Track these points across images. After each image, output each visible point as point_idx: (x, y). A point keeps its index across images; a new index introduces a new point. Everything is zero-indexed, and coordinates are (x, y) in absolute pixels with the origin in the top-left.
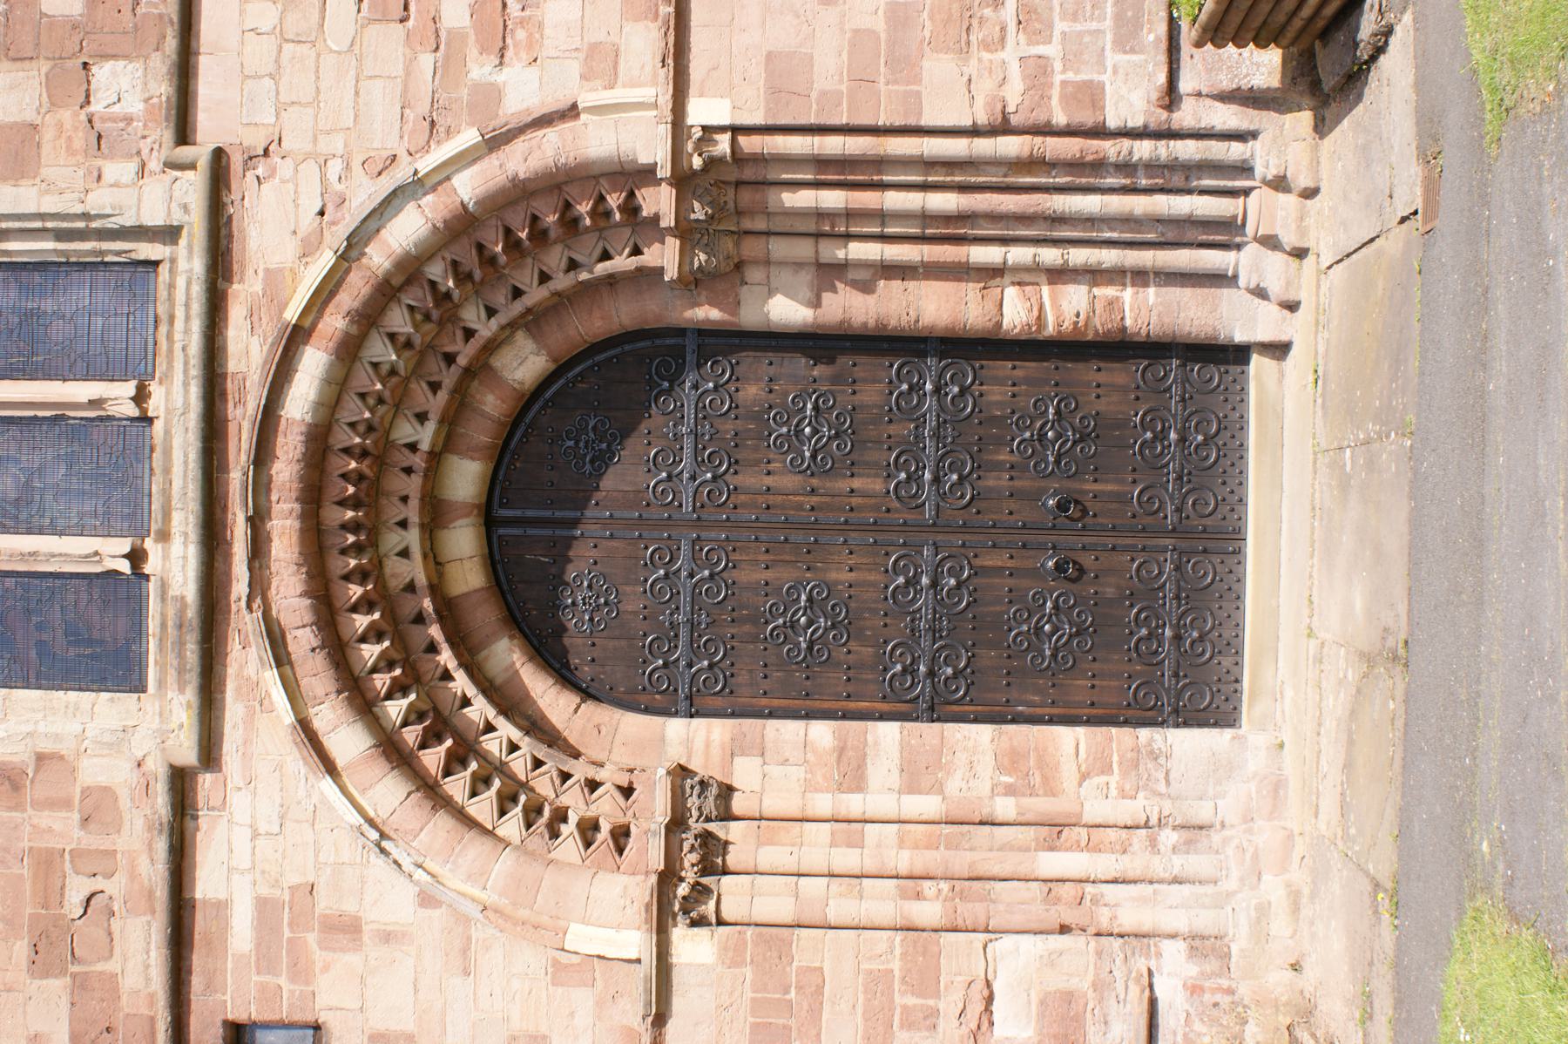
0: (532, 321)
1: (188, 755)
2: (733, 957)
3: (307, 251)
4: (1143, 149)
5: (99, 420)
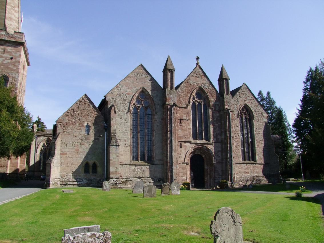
0: (205, 156)
1: (192, 142)
5: (203, 138)
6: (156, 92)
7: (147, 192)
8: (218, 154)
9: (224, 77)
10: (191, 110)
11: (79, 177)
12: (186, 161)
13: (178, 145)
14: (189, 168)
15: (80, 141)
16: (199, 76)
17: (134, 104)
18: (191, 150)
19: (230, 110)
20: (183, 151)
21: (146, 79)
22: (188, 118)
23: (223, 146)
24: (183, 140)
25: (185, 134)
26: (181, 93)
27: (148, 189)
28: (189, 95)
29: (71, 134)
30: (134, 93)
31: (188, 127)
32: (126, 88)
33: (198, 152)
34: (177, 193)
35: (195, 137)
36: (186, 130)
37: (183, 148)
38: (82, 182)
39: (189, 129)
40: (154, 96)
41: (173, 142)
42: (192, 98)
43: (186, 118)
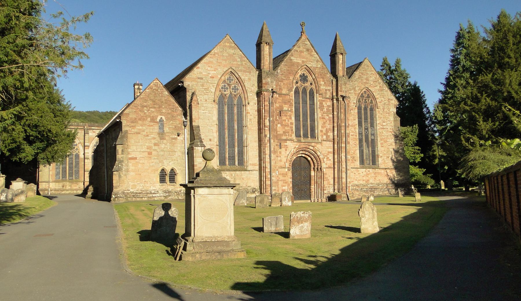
2: (286, 172)
3: (318, 148)
4: (323, 193)
6: (248, 74)
7: (259, 202)
8: (328, 156)
9: (339, 51)
10: (294, 98)
11: (154, 188)
12: (287, 165)
13: (277, 145)
14: (290, 174)
15: (153, 141)
16: (305, 50)
17: (220, 91)
18: (293, 151)
19: (345, 97)
20: (283, 153)
21: (234, 56)
22: (289, 109)
23: (336, 146)
24: (284, 138)
25: (285, 130)
26: (281, 75)
27: (260, 198)
28: (291, 78)
29: (142, 133)
30: (220, 76)
31: (290, 121)
32: (209, 69)
33: (302, 154)
34: (288, 204)
35: (298, 135)
36: (288, 126)
37: (283, 149)
38: (158, 195)
39: (292, 123)
40: (245, 79)
41: (272, 141)
42: (295, 81)
43: (287, 109)
